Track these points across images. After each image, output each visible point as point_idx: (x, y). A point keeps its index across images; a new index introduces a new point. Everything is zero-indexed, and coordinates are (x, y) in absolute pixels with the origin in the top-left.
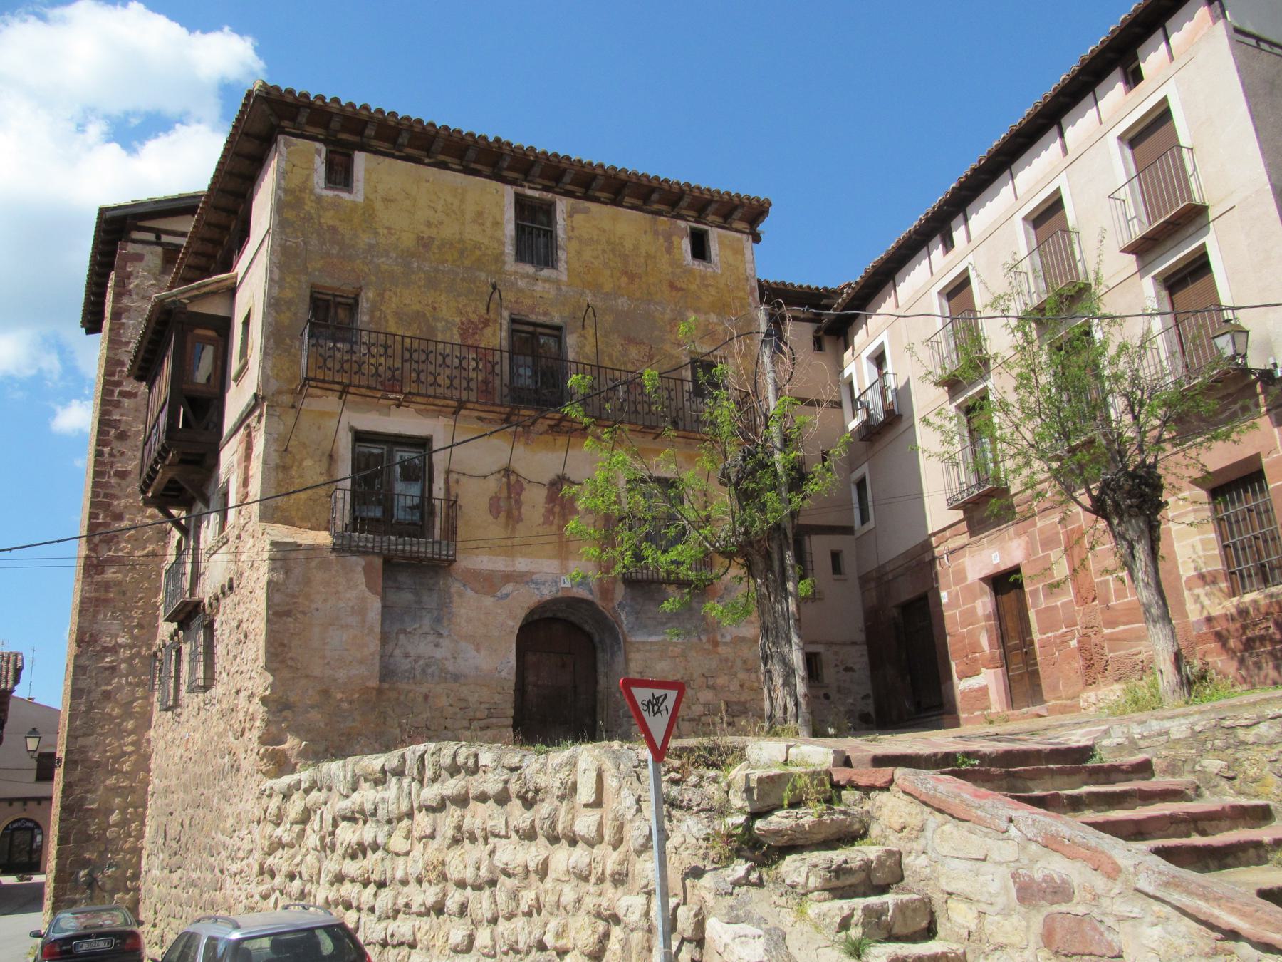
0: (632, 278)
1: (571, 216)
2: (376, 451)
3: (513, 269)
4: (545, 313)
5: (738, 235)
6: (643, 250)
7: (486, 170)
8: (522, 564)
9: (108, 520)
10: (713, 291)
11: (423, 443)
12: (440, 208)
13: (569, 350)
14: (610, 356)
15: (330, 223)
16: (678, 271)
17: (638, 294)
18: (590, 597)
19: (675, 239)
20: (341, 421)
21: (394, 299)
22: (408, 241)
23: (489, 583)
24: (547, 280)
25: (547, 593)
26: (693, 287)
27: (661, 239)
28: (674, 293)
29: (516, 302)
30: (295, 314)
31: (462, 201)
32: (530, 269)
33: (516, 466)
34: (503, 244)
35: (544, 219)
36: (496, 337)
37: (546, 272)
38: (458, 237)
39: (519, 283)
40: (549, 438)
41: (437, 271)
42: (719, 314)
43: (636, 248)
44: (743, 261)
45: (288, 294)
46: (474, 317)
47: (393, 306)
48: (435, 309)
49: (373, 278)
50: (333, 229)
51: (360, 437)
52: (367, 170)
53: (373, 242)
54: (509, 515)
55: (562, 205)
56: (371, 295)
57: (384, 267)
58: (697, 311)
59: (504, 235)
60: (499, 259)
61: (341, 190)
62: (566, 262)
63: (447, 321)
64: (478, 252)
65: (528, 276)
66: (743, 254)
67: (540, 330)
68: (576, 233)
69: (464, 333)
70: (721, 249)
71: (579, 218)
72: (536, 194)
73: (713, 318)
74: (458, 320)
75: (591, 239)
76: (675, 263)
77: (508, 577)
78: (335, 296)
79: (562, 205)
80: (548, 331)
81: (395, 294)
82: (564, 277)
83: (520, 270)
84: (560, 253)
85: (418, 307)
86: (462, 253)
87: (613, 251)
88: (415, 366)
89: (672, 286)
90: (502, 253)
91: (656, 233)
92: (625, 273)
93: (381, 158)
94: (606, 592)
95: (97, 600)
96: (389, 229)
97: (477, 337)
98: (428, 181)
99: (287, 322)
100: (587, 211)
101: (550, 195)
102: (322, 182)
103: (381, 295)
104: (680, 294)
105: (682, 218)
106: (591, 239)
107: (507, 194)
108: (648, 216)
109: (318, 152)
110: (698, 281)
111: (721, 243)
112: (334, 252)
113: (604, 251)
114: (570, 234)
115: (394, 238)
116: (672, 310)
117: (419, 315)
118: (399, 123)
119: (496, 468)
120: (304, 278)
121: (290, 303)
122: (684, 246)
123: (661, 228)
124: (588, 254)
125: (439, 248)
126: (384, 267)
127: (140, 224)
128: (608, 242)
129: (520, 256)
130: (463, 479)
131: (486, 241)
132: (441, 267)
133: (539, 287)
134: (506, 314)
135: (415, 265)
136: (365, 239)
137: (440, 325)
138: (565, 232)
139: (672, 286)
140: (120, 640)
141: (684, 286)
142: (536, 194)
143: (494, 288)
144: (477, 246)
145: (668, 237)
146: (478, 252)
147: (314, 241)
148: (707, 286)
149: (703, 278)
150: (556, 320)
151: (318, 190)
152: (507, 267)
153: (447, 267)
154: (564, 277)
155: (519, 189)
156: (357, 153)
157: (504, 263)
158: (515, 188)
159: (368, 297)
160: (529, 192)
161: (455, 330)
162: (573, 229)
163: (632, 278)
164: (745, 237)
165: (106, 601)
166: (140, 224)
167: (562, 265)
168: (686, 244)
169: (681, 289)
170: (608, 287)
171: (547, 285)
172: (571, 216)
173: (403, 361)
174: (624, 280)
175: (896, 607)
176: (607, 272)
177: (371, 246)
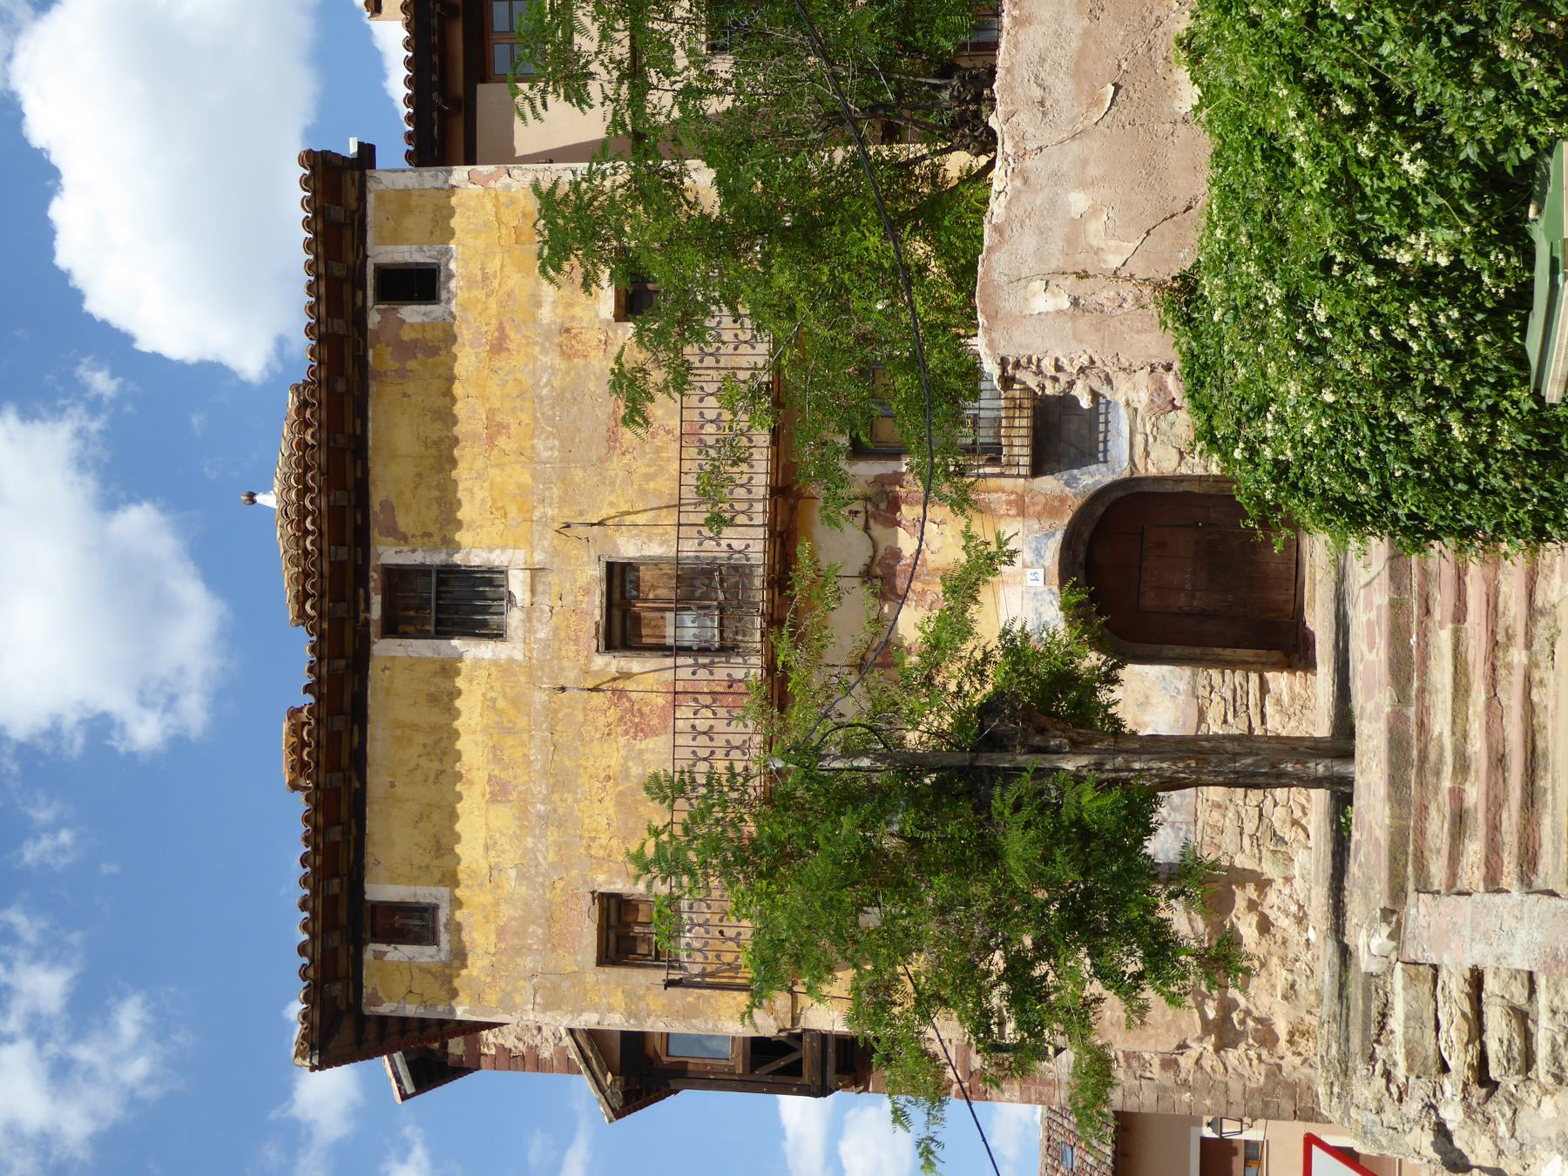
1: (404, 538)
3: (520, 646)
4: (587, 592)
5: (371, 198)
10: (494, 265)
12: (436, 766)
13: (647, 552)
14: (648, 477)
15: (493, 938)
17: (525, 418)
19: (407, 335)
21: (604, 842)
26: (493, 305)
27: (411, 364)
29: (576, 642)
31: (415, 727)
32: (514, 618)
37: (517, 584)
38: (480, 738)
39: (541, 635)
44: (422, 193)
46: (613, 714)
49: (574, 872)
50: (501, 933)
52: (393, 881)
53: (513, 873)
55: (387, 553)
56: (601, 878)
57: (552, 857)
58: (539, 305)
60: (506, 669)
61: (435, 918)
62: (491, 550)
63: (626, 759)
64: (501, 704)
65: (528, 618)
66: (406, 192)
67: (617, 596)
68: (433, 529)
69: (641, 730)
70: (406, 241)
71: (404, 522)
72: (376, 600)
74: (622, 740)
75: (439, 501)
79: (387, 553)
80: (617, 581)
81: (593, 839)
83: (521, 632)
85: (610, 805)
86: (509, 732)
90: (495, 662)
91: (402, 374)
92: (491, 439)
93: (369, 860)
94: (1051, 509)
96: (487, 848)
97: (646, 710)
98: (392, 785)
100: (388, 507)
101: (374, 575)
102: (430, 950)
104: (512, 334)
105: (360, 317)
106: (439, 501)
107: (384, 649)
108: (373, 388)
109: (379, 956)
110: (479, 294)
112: (540, 931)
114: (437, 539)
116: (544, 351)
118: (316, 849)
121: (631, 996)
122: (418, 319)
123: (392, 364)
125: (504, 769)
126: (552, 857)
132: (538, 766)
135: (540, 807)
137: (635, 770)
138: (435, 549)
142: (376, 600)
145: (407, 349)
147: (528, 962)
148: (485, 277)
151: (443, 956)
152: (519, 656)
153: (534, 754)
155: (373, 629)
156: (367, 897)
157: (511, 660)
158: (373, 638)
160: (376, 612)
161: (640, 745)
162: (428, 535)
164: (371, 185)
167: (497, 559)
168: (412, 314)
169: (501, 328)
171: (540, 588)
172: (404, 538)
174: (502, 441)
176: (492, 471)
177: (522, 876)
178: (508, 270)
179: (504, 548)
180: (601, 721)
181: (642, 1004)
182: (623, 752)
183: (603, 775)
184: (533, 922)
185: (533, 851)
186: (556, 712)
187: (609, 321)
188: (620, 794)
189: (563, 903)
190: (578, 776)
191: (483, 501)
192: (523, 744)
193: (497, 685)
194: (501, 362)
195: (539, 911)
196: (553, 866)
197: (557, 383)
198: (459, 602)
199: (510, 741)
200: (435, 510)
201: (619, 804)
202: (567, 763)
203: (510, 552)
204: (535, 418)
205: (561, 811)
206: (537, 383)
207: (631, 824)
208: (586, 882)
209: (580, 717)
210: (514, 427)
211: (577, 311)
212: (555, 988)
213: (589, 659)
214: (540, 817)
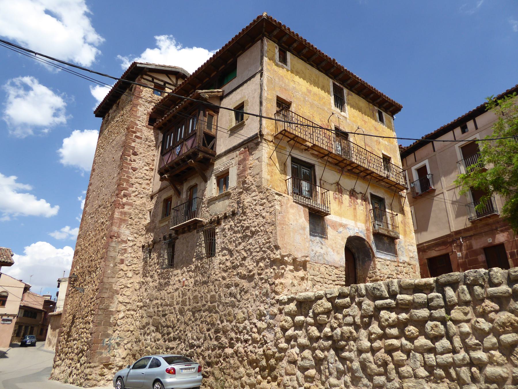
2: (295, 166)
7: (324, 71)
8: (344, 221)
9: (127, 187)
11: (311, 167)
18: (364, 237)
23: (336, 226)
25: (352, 234)
33: (340, 182)
51: (294, 160)
54: (339, 201)
57: (298, 96)
77: (341, 225)
85: (308, 114)
88: (316, 135)
95: (121, 219)
119: (334, 182)
127: (148, 73)
140: (129, 238)
143: (333, 114)
165: (125, 220)
166: (148, 73)
175: (427, 259)
196: (296, 96)
198: (340, 102)
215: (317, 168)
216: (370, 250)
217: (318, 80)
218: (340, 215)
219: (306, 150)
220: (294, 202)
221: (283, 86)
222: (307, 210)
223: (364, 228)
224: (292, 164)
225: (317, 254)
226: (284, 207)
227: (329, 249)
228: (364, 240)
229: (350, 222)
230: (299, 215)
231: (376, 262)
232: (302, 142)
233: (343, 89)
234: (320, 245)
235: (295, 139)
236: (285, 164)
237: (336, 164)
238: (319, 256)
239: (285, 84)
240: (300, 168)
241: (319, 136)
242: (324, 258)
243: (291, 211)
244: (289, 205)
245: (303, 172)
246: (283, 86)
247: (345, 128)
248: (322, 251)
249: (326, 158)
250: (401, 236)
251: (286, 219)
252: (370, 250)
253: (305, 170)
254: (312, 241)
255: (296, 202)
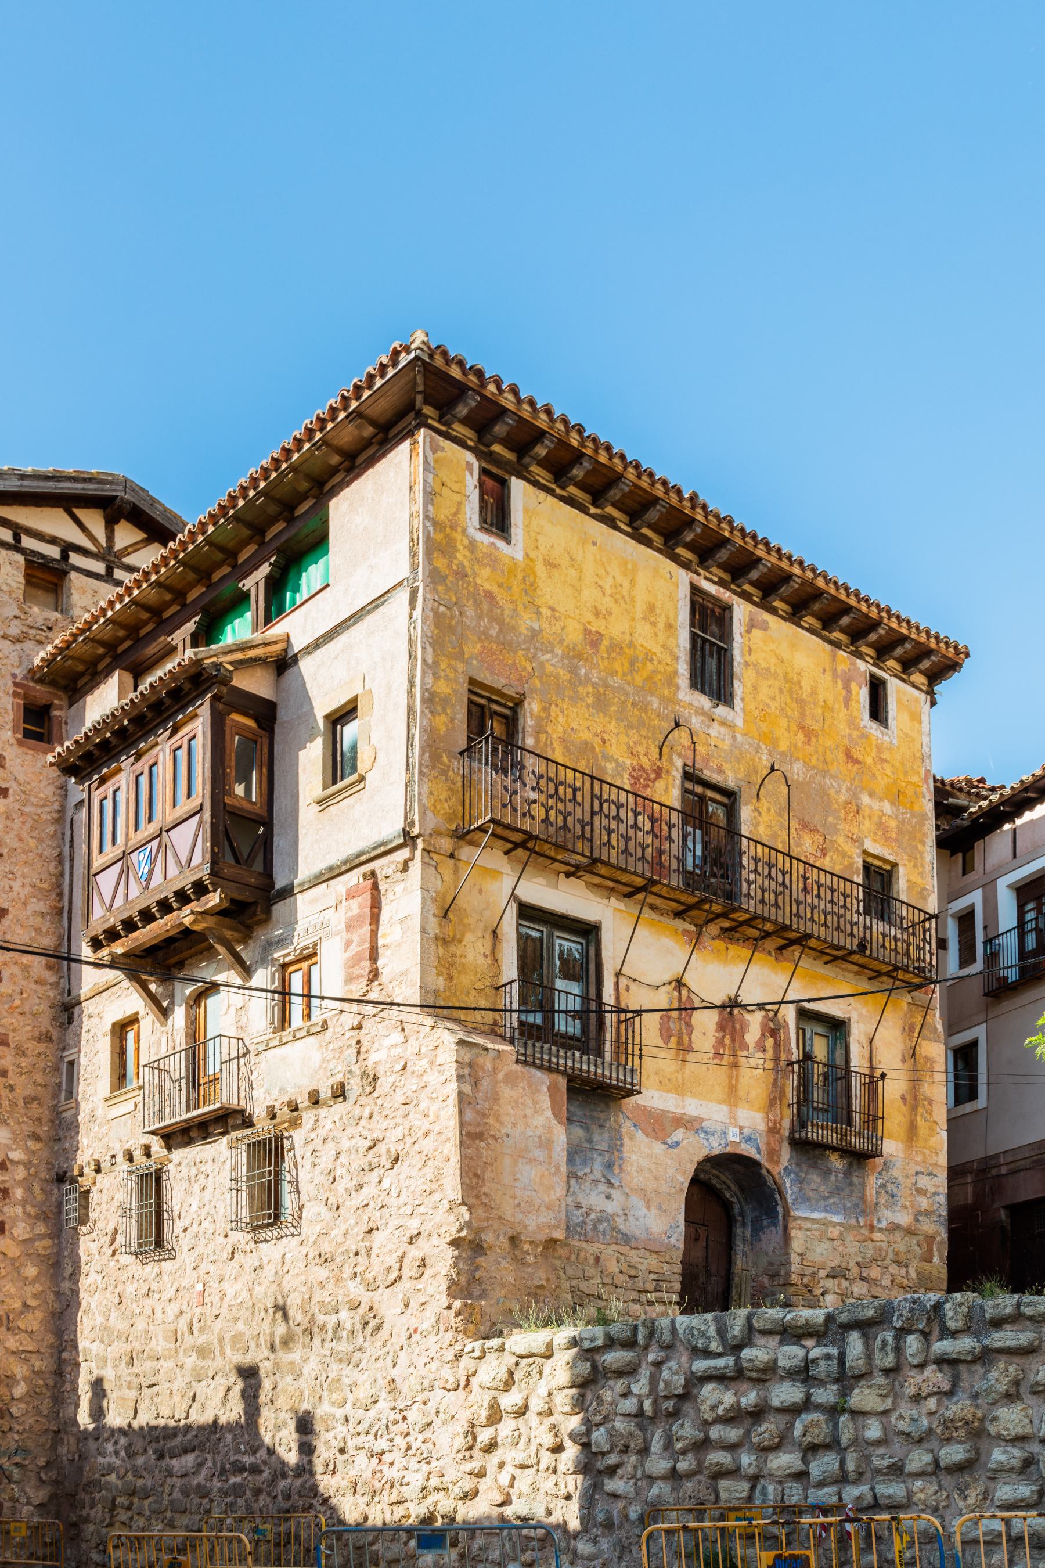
0: (809, 735)
2: (535, 934)
6: (821, 698)
16: (855, 734)
17: (814, 762)
20: (501, 885)
22: (574, 635)
24: (723, 723)
27: (840, 685)
28: (850, 765)
30: (452, 720)
34: (677, 659)
35: (714, 628)
36: (669, 792)
37: (722, 710)
39: (694, 720)
40: (719, 944)
41: (606, 686)
42: (892, 803)
43: (814, 693)
45: (443, 688)
46: (645, 762)
47: (560, 729)
48: (604, 742)
49: (538, 684)
51: (528, 912)
58: (871, 795)
59: (678, 645)
60: (671, 680)
62: (743, 699)
63: (616, 761)
64: (650, 667)
65: (704, 713)
67: (710, 793)
73: (887, 807)
74: (628, 762)
75: (768, 669)
76: (852, 723)
78: (490, 700)
80: (718, 797)
82: (739, 722)
84: (736, 683)
85: (586, 735)
86: (632, 663)
87: (791, 691)
89: (849, 756)
99: (443, 730)
103: (545, 709)
106: (768, 669)
111: (899, 702)
113: (781, 691)
115: (557, 627)
116: (848, 790)
117: (587, 747)
120: (460, 667)
124: (764, 692)
126: (549, 668)
128: (787, 680)
129: (699, 680)
130: (633, 987)
131: (657, 649)
133: (715, 730)
134: (679, 763)
135: (583, 672)
136: (526, 621)
137: (610, 767)
138: (743, 655)
139: (849, 756)
141: (861, 758)
143: (677, 725)
144: (649, 657)
146: (650, 667)
148: (883, 761)
149: (879, 748)
150: (730, 781)
154: (739, 722)
159: (532, 707)
161: (626, 776)
163: (809, 735)
169: (857, 762)
170: (783, 746)
171: (723, 729)
173: (593, 813)
174: (801, 737)
177: (535, 634)
178: (886, 780)
179: (744, 710)
180: (641, 750)
181: (439, 708)
182: (621, 760)
183: (606, 737)
184: (501, 631)
185: (552, 651)
186: (646, 712)
187: (862, 844)
188: (593, 747)
189: (514, 664)
190: (605, 714)
191: (768, 706)
192: (624, 675)
193: (661, 668)
194: (841, 757)
195: (508, 638)
196: (542, 665)
197: (832, 792)
199: (626, 664)
200: (764, 665)
201: (587, 743)
202: (613, 709)
203: (741, 714)
204: (814, 768)
205: (580, 689)
206: (832, 777)
207: (572, 748)
208: (531, 691)
209: (643, 733)
210: (809, 749)
211: (867, 823)
212: (452, 630)
213: (680, 755)
214: (576, 668)
215: (607, 937)
216: (777, 1196)
217: (633, 583)
218: (680, 1090)
219: (568, 875)
220: (518, 1061)
221: (494, 633)
222: (562, 1082)
223: (762, 1127)
224: (518, 925)
225: (593, 1216)
226: (485, 1083)
227: (635, 1200)
228: (757, 1164)
229: (711, 1111)
230: (535, 1103)
231: (793, 1233)
232: (552, 854)
233: (727, 608)
234: (602, 1187)
235: (530, 845)
236: (494, 932)
237: (678, 915)
238: (600, 1220)
239: (501, 622)
240: (551, 936)
241: (613, 825)
242: (614, 1229)
243: (507, 1093)
244: (500, 1076)
245: (561, 952)
246: (494, 633)
247: (726, 767)
248: (611, 1207)
249: (641, 896)
250: (891, 1147)
251: (491, 1121)
252: (777, 1196)
253: (566, 945)
254: (577, 1177)
255: (525, 1063)
